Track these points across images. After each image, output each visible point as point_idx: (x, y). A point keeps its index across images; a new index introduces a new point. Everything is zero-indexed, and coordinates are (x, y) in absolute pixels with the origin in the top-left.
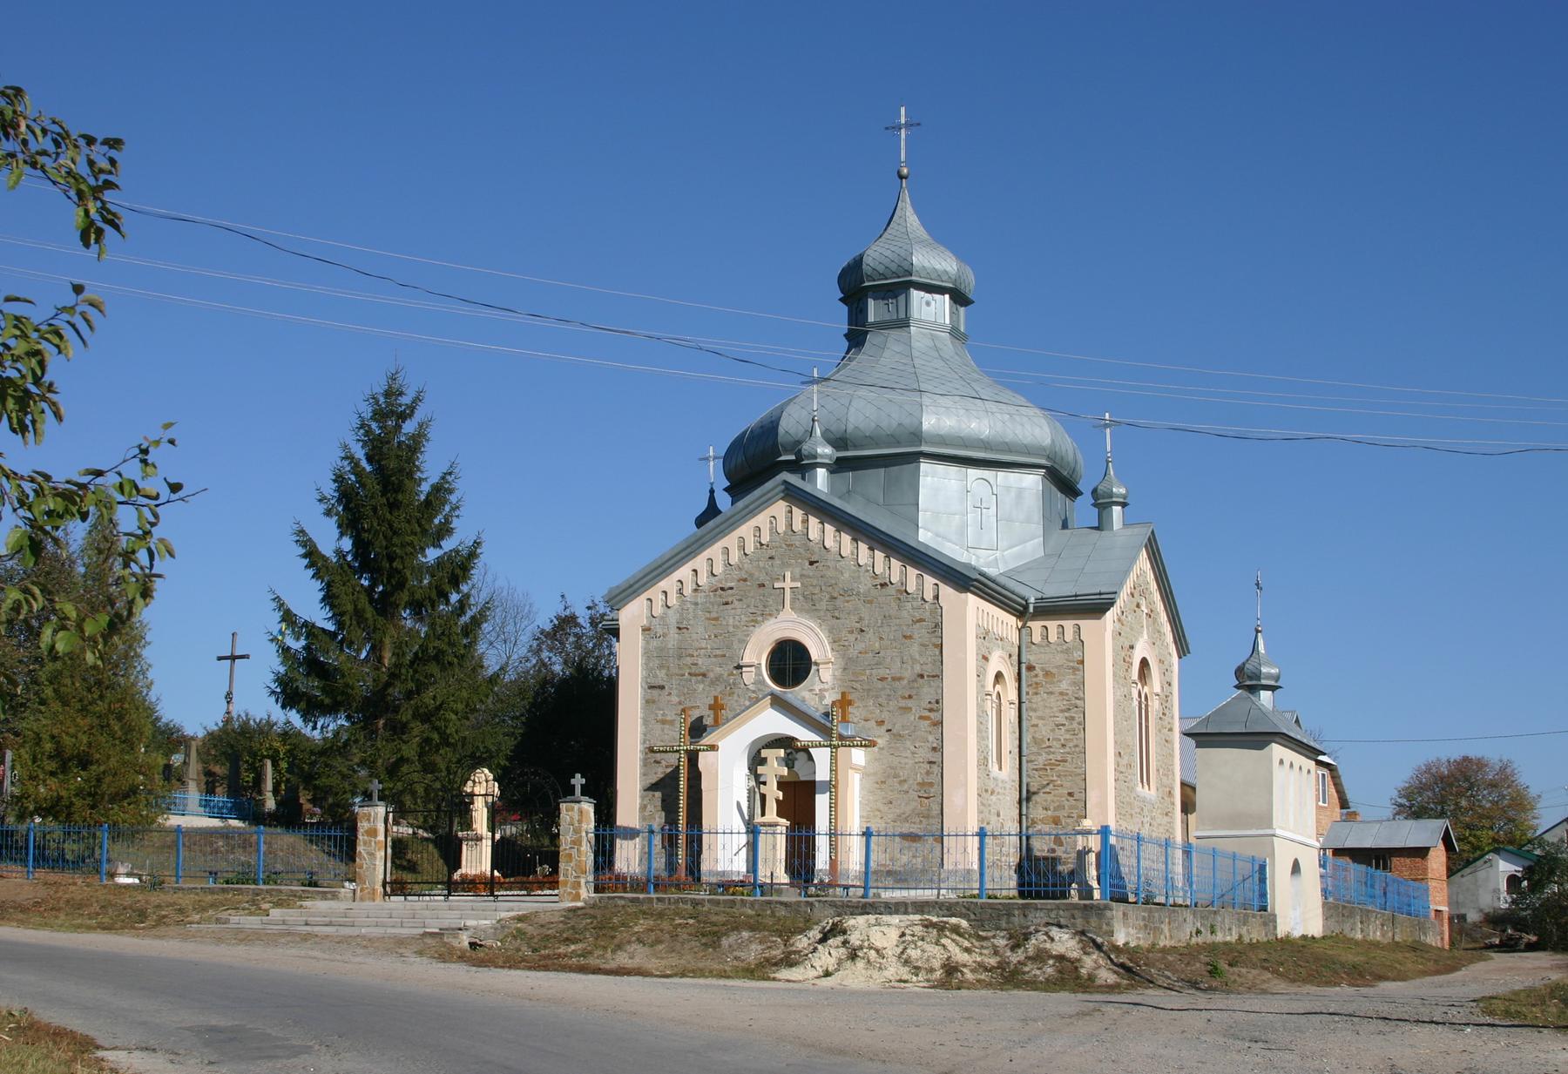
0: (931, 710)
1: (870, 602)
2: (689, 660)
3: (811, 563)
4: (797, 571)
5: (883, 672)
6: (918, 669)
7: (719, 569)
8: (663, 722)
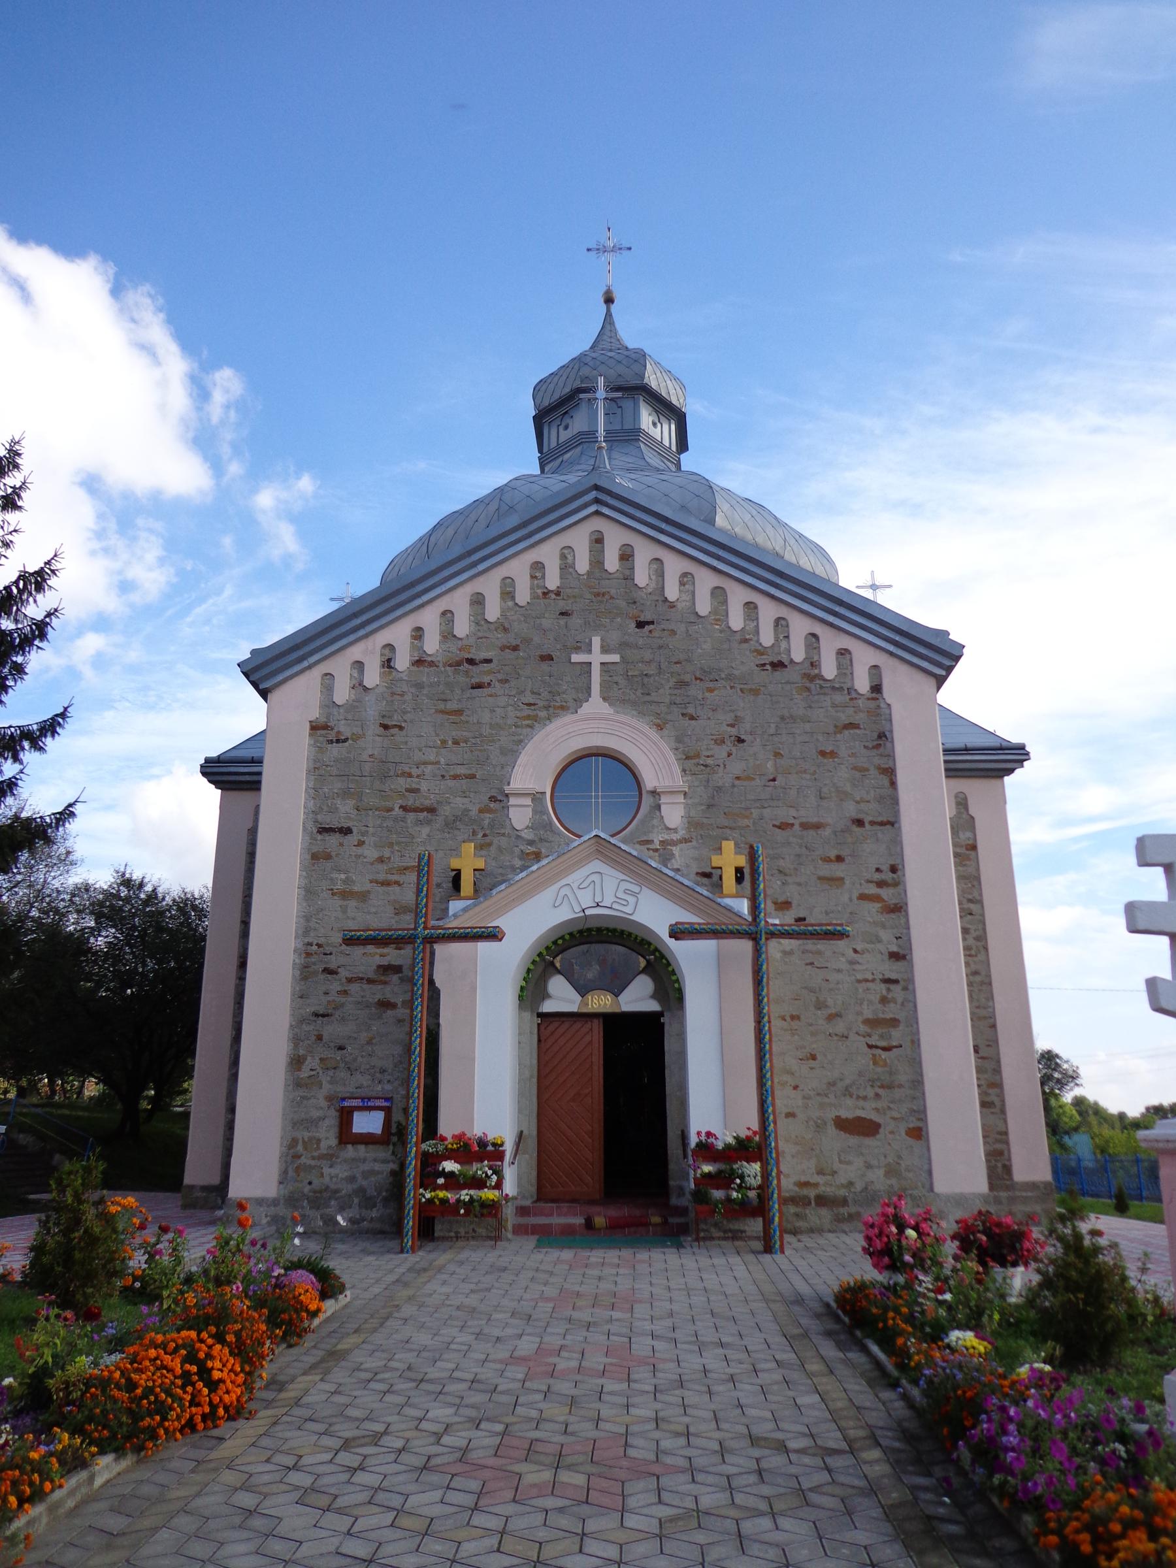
0: (881, 884)
1: (755, 692)
2: (402, 783)
3: (640, 625)
4: (615, 637)
5: (784, 814)
6: (851, 810)
7: (462, 627)
8: (345, 895)
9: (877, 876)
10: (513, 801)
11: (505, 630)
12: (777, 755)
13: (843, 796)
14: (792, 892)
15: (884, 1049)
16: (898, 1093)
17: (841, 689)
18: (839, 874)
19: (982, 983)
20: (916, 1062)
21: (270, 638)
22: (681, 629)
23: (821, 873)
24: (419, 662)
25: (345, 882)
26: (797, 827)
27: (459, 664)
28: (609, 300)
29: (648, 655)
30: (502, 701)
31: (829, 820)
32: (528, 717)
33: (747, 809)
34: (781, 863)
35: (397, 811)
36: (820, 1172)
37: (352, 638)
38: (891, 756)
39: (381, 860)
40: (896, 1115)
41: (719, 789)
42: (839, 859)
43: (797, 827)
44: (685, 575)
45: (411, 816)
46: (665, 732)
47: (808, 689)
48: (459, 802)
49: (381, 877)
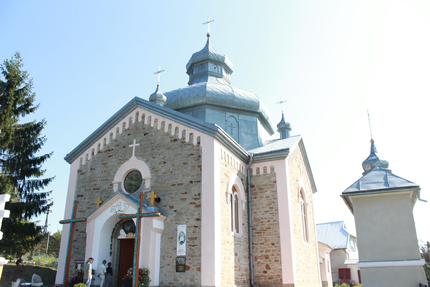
0: (195, 199)
1: (169, 148)
2: (94, 183)
3: (145, 135)
4: (139, 139)
5: (174, 181)
6: (190, 179)
9: (195, 197)
10: (114, 185)
11: (117, 141)
12: (173, 165)
13: (188, 175)
14: (173, 204)
15: (193, 246)
16: (195, 258)
17: (190, 144)
18: (185, 197)
19: (276, 224)
20: (200, 249)
21: (68, 152)
22: (153, 134)
23: (181, 197)
24: (99, 152)
25: (81, 208)
26: (176, 185)
27: (107, 151)
28: (208, 36)
29: (146, 142)
30: (114, 159)
31: (185, 183)
32: (119, 163)
33: (165, 181)
34: (172, 195)
35: (92, 190)
36: (174, 280)
37: (86, 148)
38: (201, 162)
39: (88, 202)
40: (194, 264)
41: (159, 177)
42: (186, 193)
43: (176, 185)
44: (156, 119)
45: (95, 191)
46: (148, 163)
47: (182, 146)
48: (104, 186)
49: (88, 207)
